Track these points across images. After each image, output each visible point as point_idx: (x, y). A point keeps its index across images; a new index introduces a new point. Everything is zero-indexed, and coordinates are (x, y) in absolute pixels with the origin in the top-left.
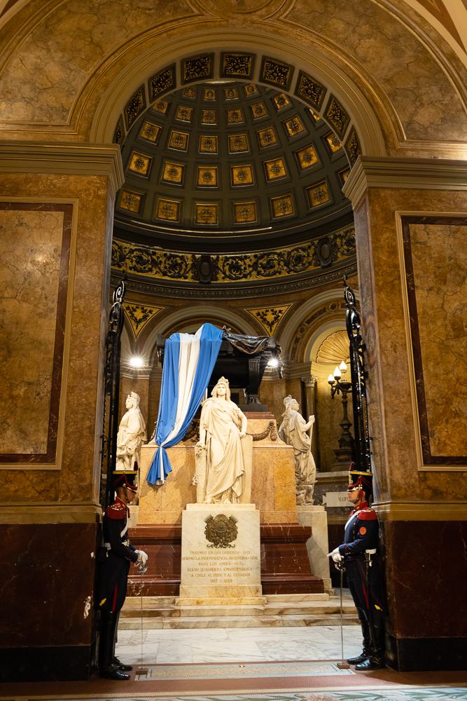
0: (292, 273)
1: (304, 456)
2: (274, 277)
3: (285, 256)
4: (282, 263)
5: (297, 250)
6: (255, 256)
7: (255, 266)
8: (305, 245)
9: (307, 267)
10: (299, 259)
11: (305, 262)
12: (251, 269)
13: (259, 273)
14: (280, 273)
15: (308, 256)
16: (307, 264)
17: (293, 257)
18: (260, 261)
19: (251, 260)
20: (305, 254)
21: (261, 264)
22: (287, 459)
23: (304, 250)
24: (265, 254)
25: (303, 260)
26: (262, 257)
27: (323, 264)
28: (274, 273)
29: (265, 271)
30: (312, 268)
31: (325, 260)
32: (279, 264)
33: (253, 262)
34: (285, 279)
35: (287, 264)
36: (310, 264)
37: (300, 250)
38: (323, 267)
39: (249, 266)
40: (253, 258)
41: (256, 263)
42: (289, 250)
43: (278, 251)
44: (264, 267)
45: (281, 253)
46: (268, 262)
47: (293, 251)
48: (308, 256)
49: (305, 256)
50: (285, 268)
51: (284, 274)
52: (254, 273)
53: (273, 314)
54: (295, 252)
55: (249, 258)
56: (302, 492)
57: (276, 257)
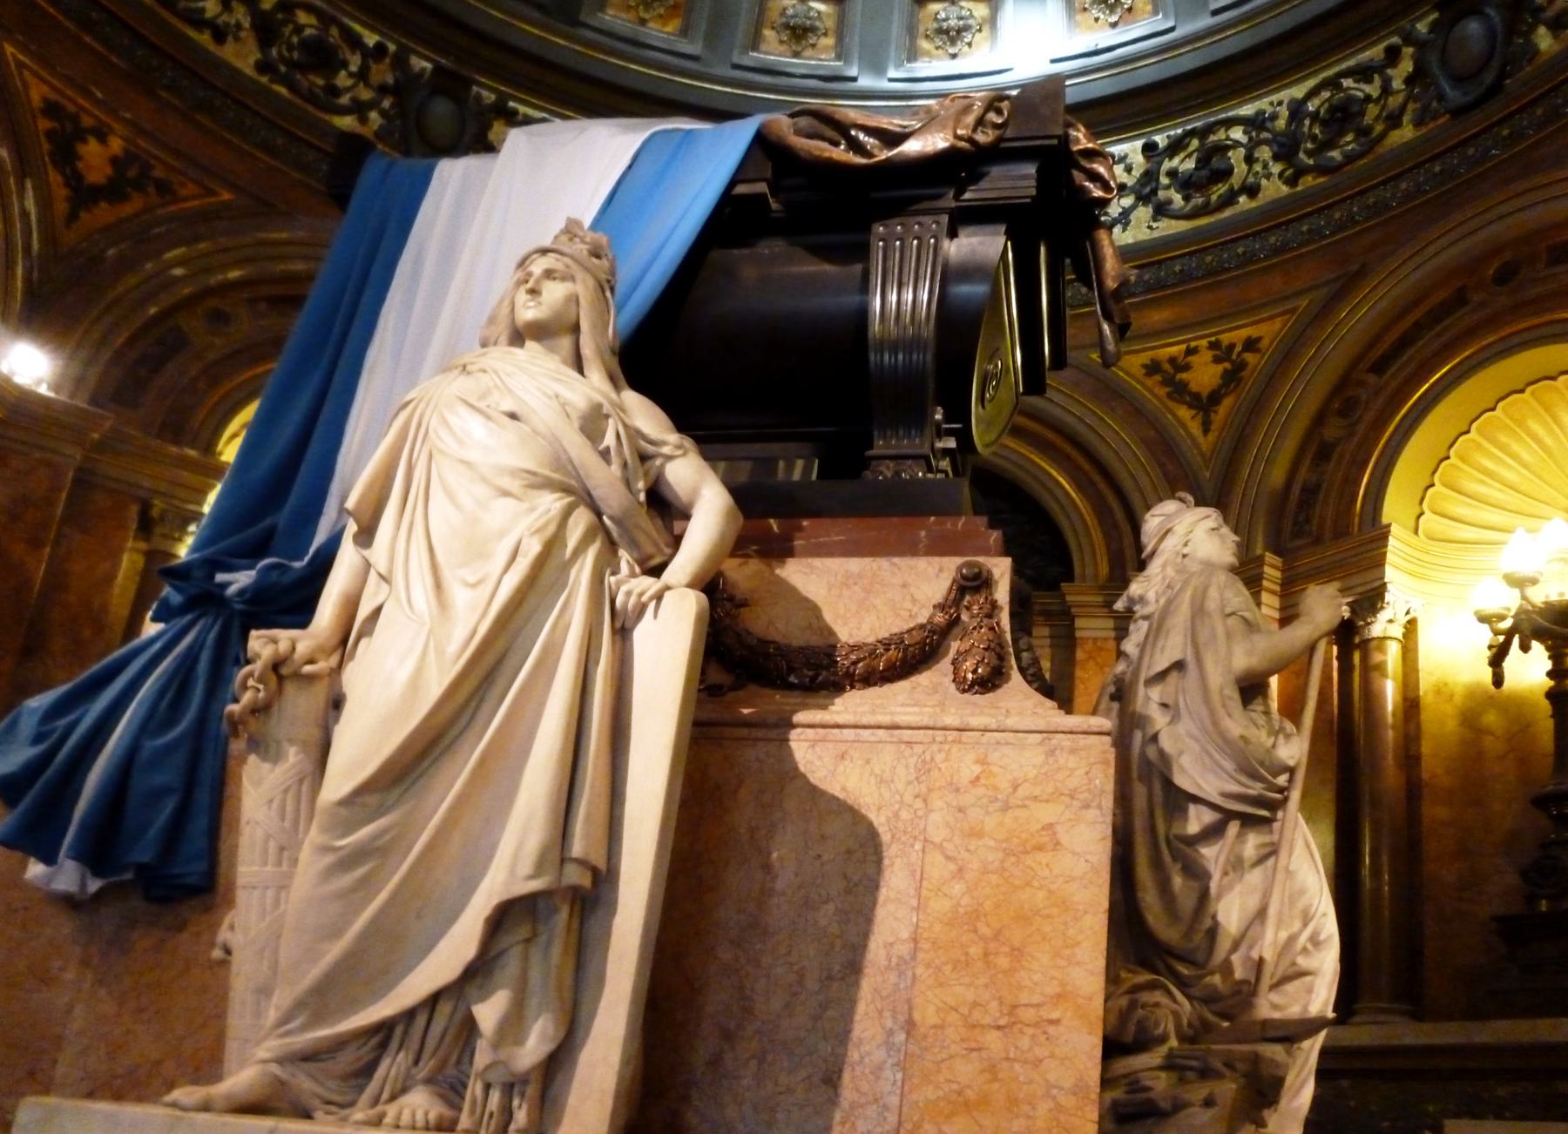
0: (1308, 181)
1: (1252, 843)
2: (1227, 213)
3: (1281, 123)
4: (1265, 153)
5: (1333, 83)
6: (1149, 149)
7: (1146, 190)
8: (1375, 53)
9: (1383, 135)
10: (1343, 116)
11: (1368, 119)
12: (1127, 201)
13: (1162, 210)
14: (1252, 191)
15: (1386, 90)
16: (1379, 128)
17: (1315, 117)
18: (1167, 165)
19: (1129, 170)
20: (1373, 89)
21: (1172, 174)
22: (1045, 813)
23: (1363, 73)
24: (1191, 133)
25: (1362, 114)
26: (1175, 147)
27: (1454, 95)
28: (1230, 199)
29: (1187, 199)
30: (1406, 133)
31: (1458, 80)
32: (1249, 160)
33: (1136, 173)
34: (1278, 206)
35: (1286, 150)
36: (1394, 121)
37: (1347, 83)
38: (1458, 112)
39: (1122, 187)
40: (1138, 159)
41: (1150, 176)
42: (1298, 92)
43: (1247, 110)
44: (1186, 184)
45: (1261, 113)
46: (1203, 162)
47: (1312, 94)
48: (1386, 90)
49: (1368, 99)
50: (1276, 168)
51: (1274, 189)
52: (1143, 213)
53: (1217, 360)
54: (1326, 94)
55: (1123, 159)
56: (1199, 1092)
57: (1237, 134)
